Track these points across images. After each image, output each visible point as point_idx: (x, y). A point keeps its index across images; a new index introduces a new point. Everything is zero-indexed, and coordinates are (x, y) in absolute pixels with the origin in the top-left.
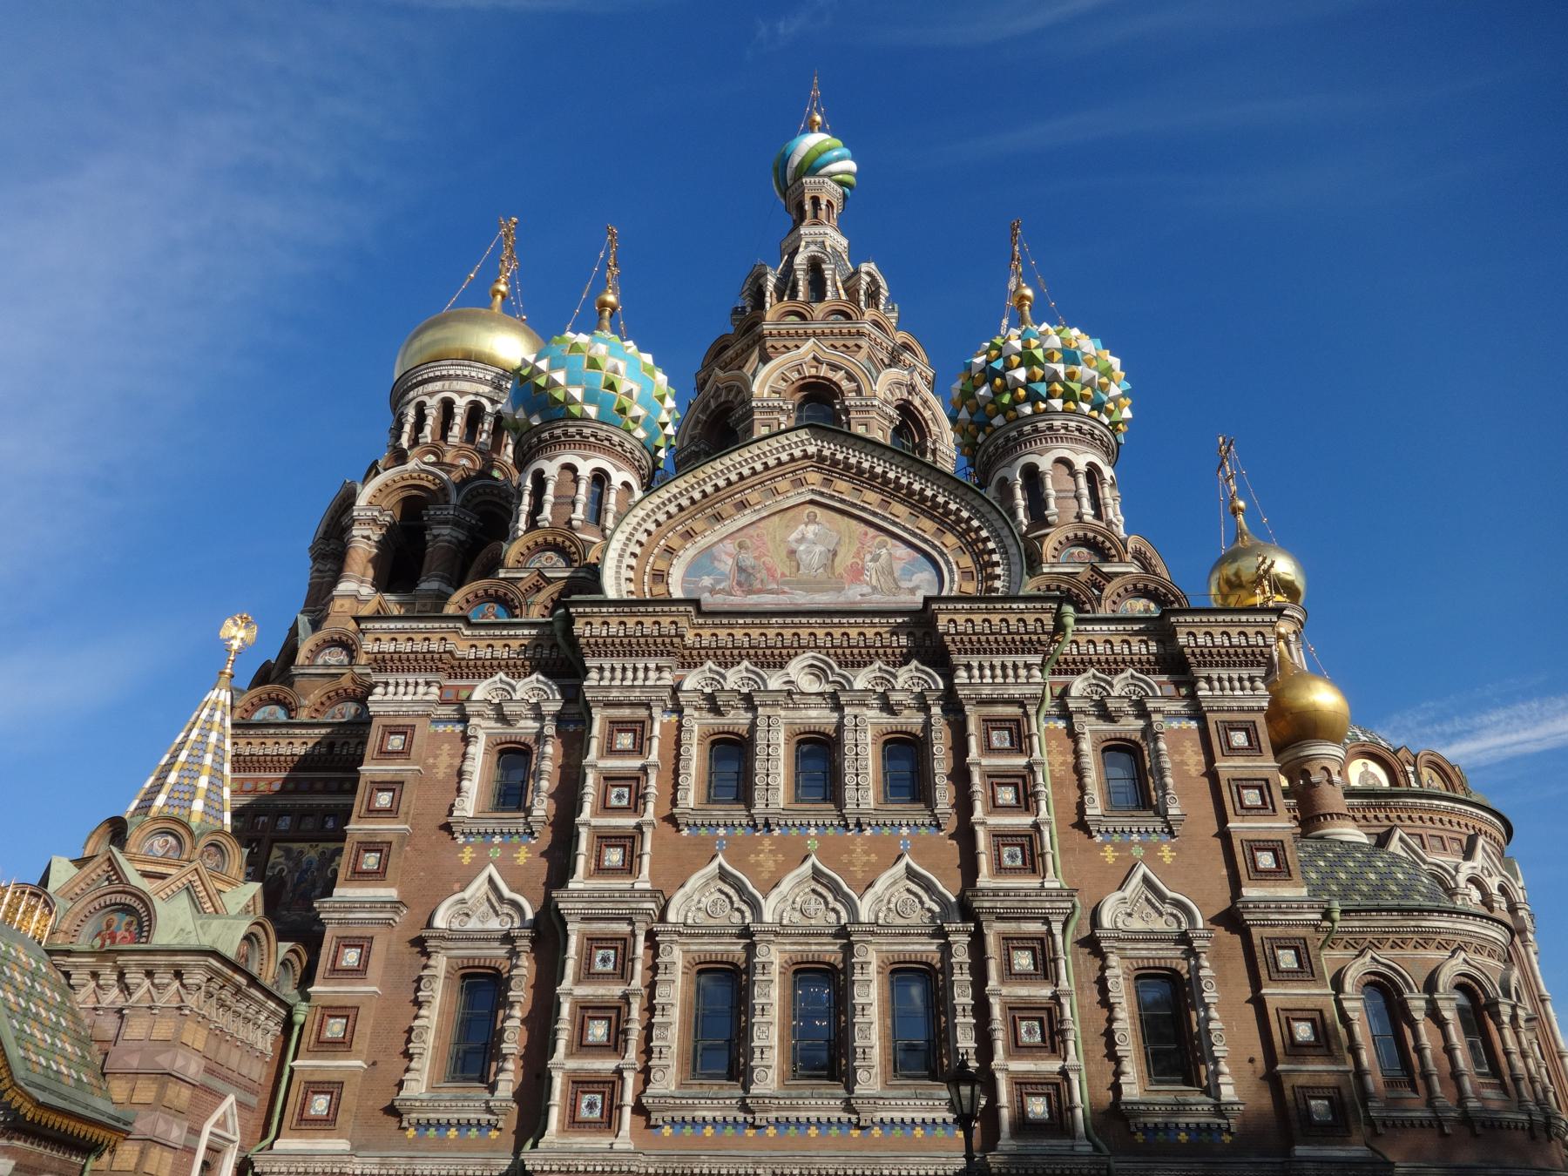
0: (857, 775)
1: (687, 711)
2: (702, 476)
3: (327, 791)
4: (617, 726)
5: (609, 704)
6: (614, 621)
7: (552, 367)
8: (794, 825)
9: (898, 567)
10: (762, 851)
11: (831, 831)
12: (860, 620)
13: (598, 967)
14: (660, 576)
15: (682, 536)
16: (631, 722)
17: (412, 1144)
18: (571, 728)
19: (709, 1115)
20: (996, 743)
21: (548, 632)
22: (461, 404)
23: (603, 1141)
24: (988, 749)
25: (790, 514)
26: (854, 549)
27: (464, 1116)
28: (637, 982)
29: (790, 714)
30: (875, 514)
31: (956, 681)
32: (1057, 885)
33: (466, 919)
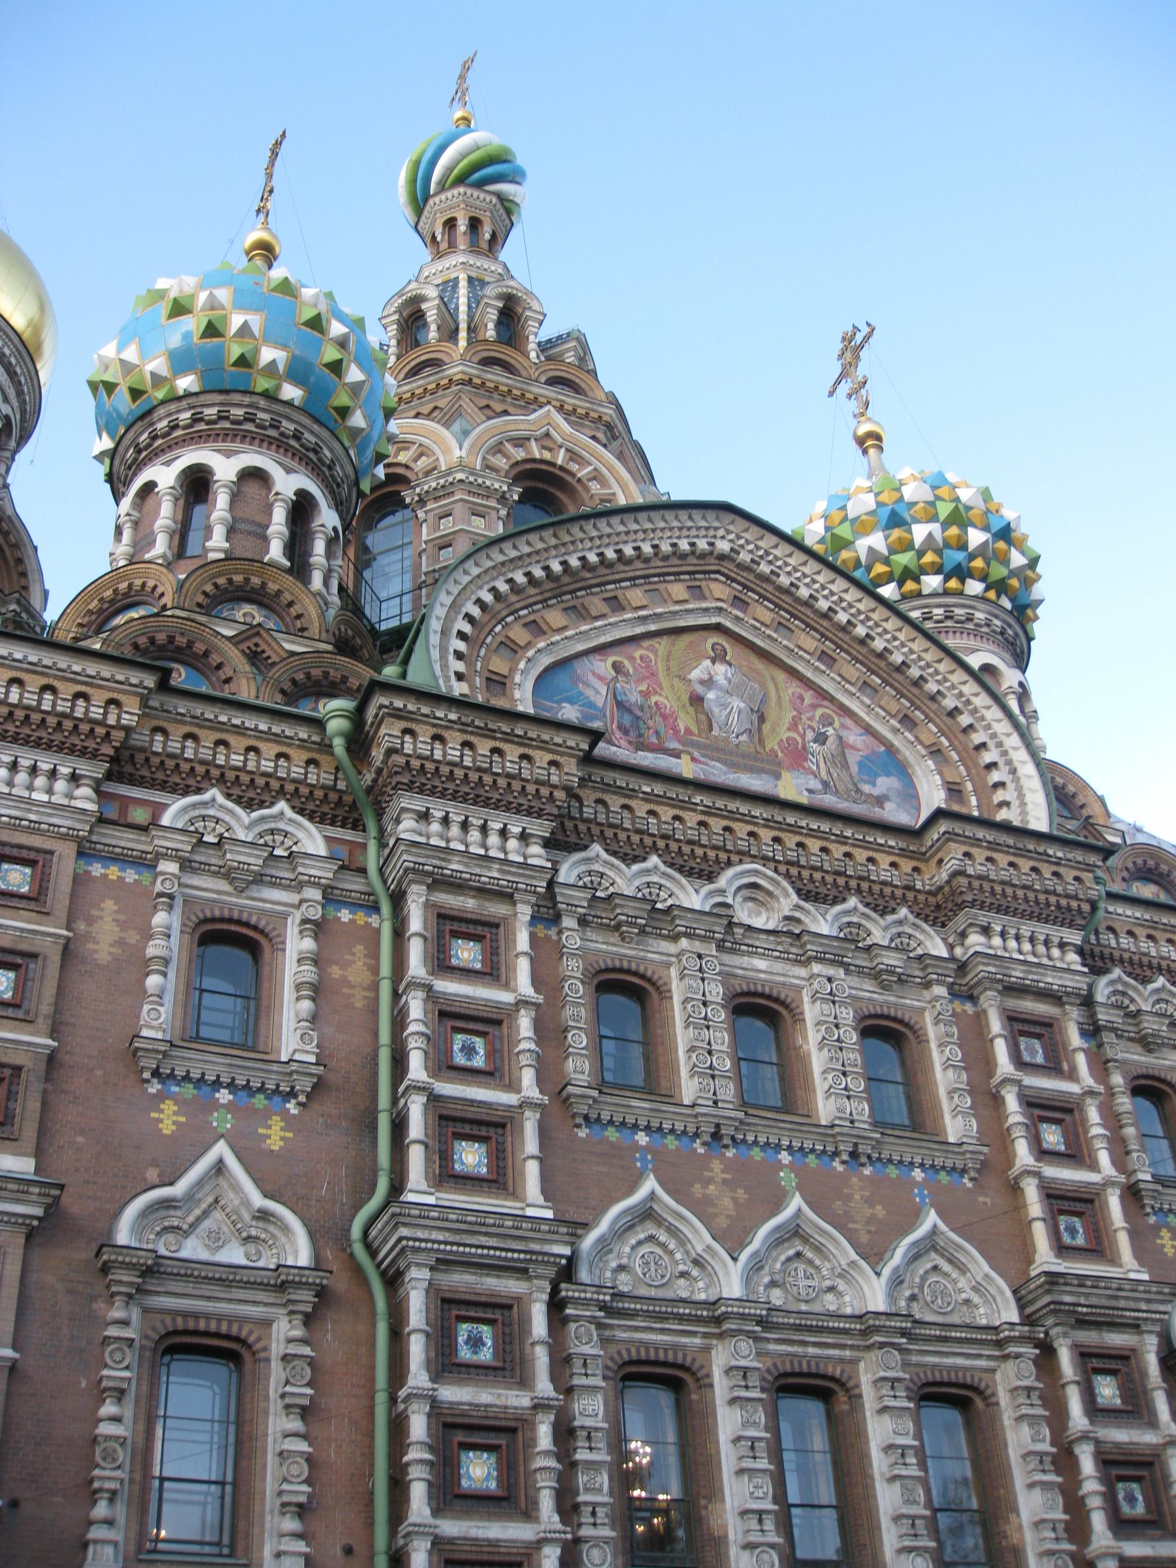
0: (844, 1074)
1: (568, 922)
2: (568, 538)
5: (440, 882)
6: (454, 739)
7: (240, 307)
8: (756, 1143)
9: (853, 759)
10: (708, 1182)
11: (811, 1160)
12: (825, 827)
13: (465, 1354)
14: (497, 682)
15: (525, 625)
16: (476, 922)
18: (345, 915)
21: (303, 735)
25: (686, 639)
28: (544, 1386)
29: (727, 958)
30: (817, 668)
33: (170, 1237)
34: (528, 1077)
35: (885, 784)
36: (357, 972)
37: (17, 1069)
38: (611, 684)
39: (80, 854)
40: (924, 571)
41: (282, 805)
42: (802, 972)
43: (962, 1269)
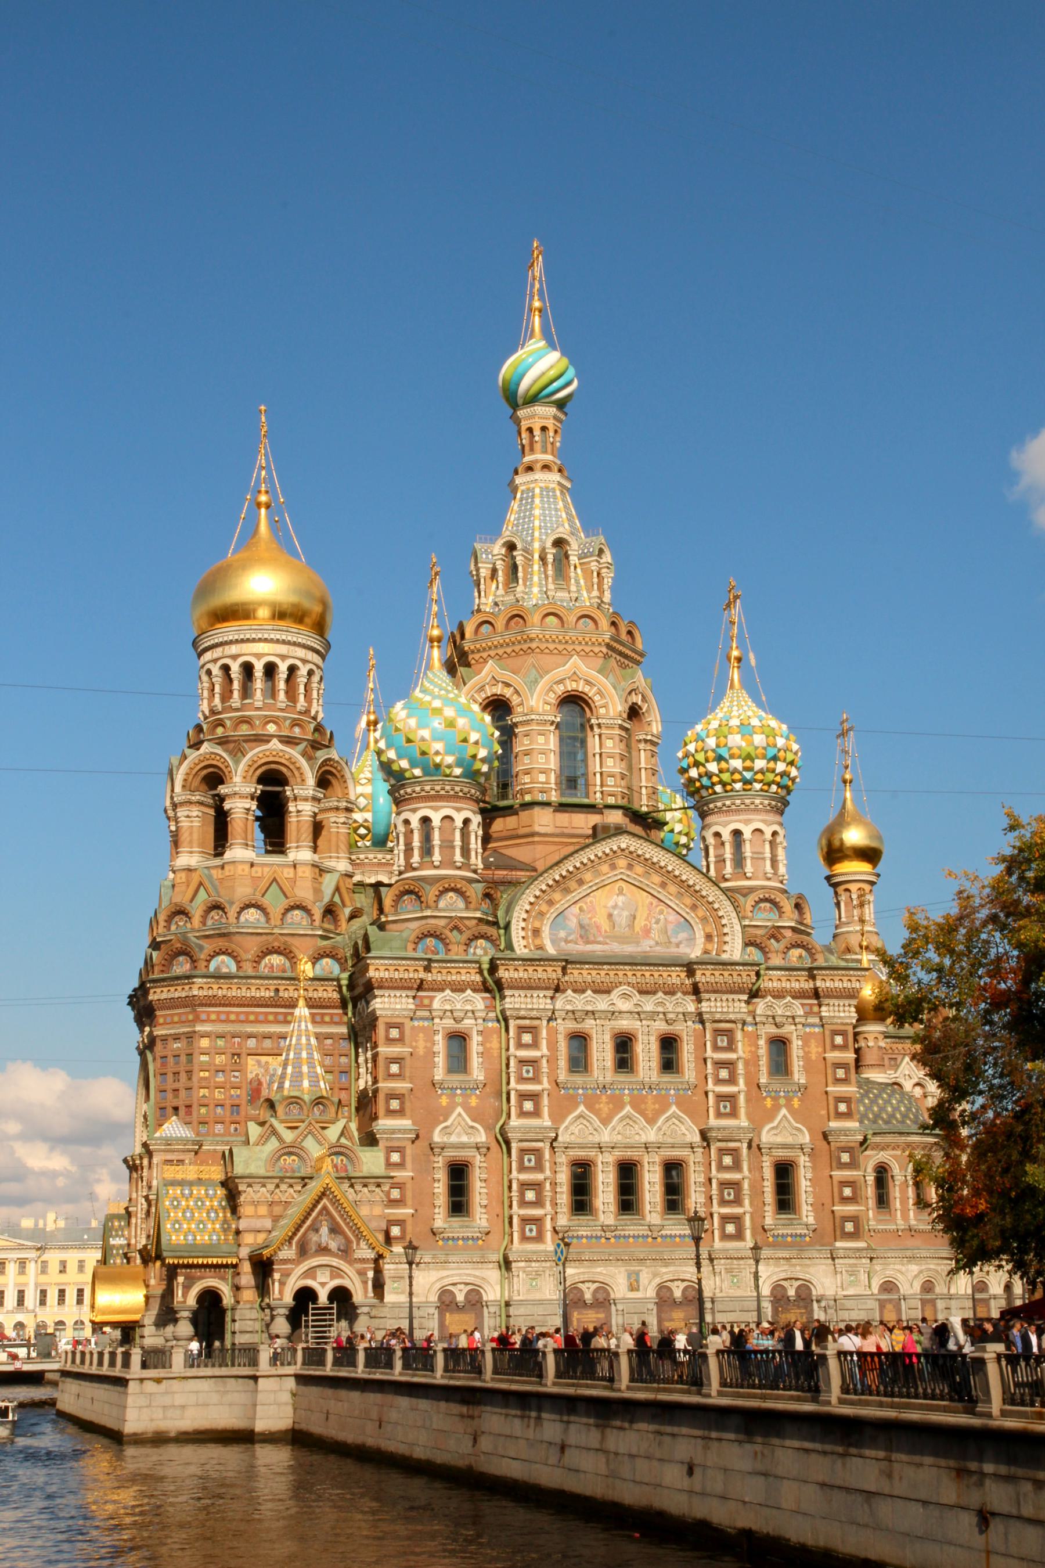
1: (559, 1021)
3: (277, 1022)
4: (522, 1029)
9: (670, 927)
13: (527, 1164)
14: (536, 932)
17: (442, 1248)
18: (490, 1024)
19: (585, 1233)
20: (720, 1044)
22: (283, 667)
23: (540, 1247)
24: (716, 1048)
26: (645, 915)
27: (465, 1235)
28: (548, 1173)
31: (703, 1010)
32: (746, 1124)
34: (545, 1080)
35: (682, 936)
36: (495, 1044)
37: (403, 1095)
38: (577, 917)
39: (412, 1019)
40: (734, 781)
41: (469, 991)
42: (639, 1023)
43: (682, 1123)
